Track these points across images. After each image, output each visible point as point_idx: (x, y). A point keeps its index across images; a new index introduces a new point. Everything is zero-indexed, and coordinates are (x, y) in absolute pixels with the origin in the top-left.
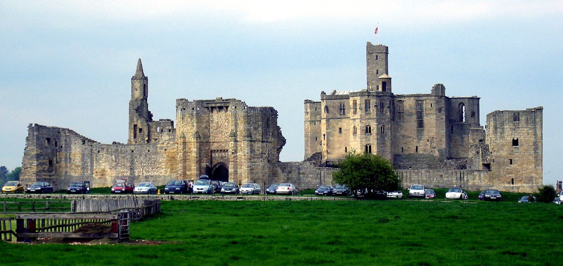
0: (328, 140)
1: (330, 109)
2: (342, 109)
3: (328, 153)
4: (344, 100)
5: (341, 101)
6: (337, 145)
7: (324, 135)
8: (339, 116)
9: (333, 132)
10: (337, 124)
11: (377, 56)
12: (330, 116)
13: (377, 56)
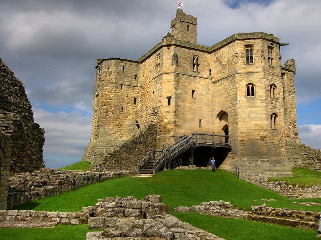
0: (177, 106)
1: (180, 59)
2: (195, 64)
3: (176, 126)
4: (197, 52)
5: (194, 51)
6: (189, 116)
7: (169, 99)
8: (191, 73)
9: (184, 95)
10: (190, 83)
11: (188, 26)
12: (180, 70)
13: (188, 26)
